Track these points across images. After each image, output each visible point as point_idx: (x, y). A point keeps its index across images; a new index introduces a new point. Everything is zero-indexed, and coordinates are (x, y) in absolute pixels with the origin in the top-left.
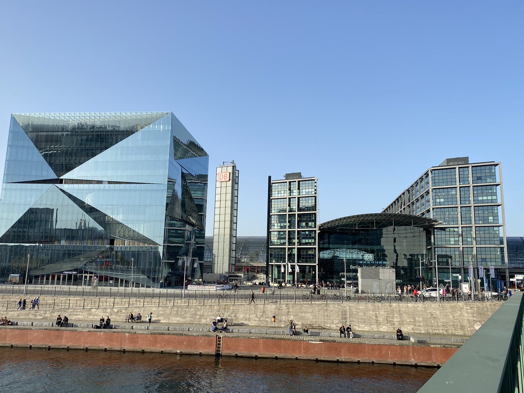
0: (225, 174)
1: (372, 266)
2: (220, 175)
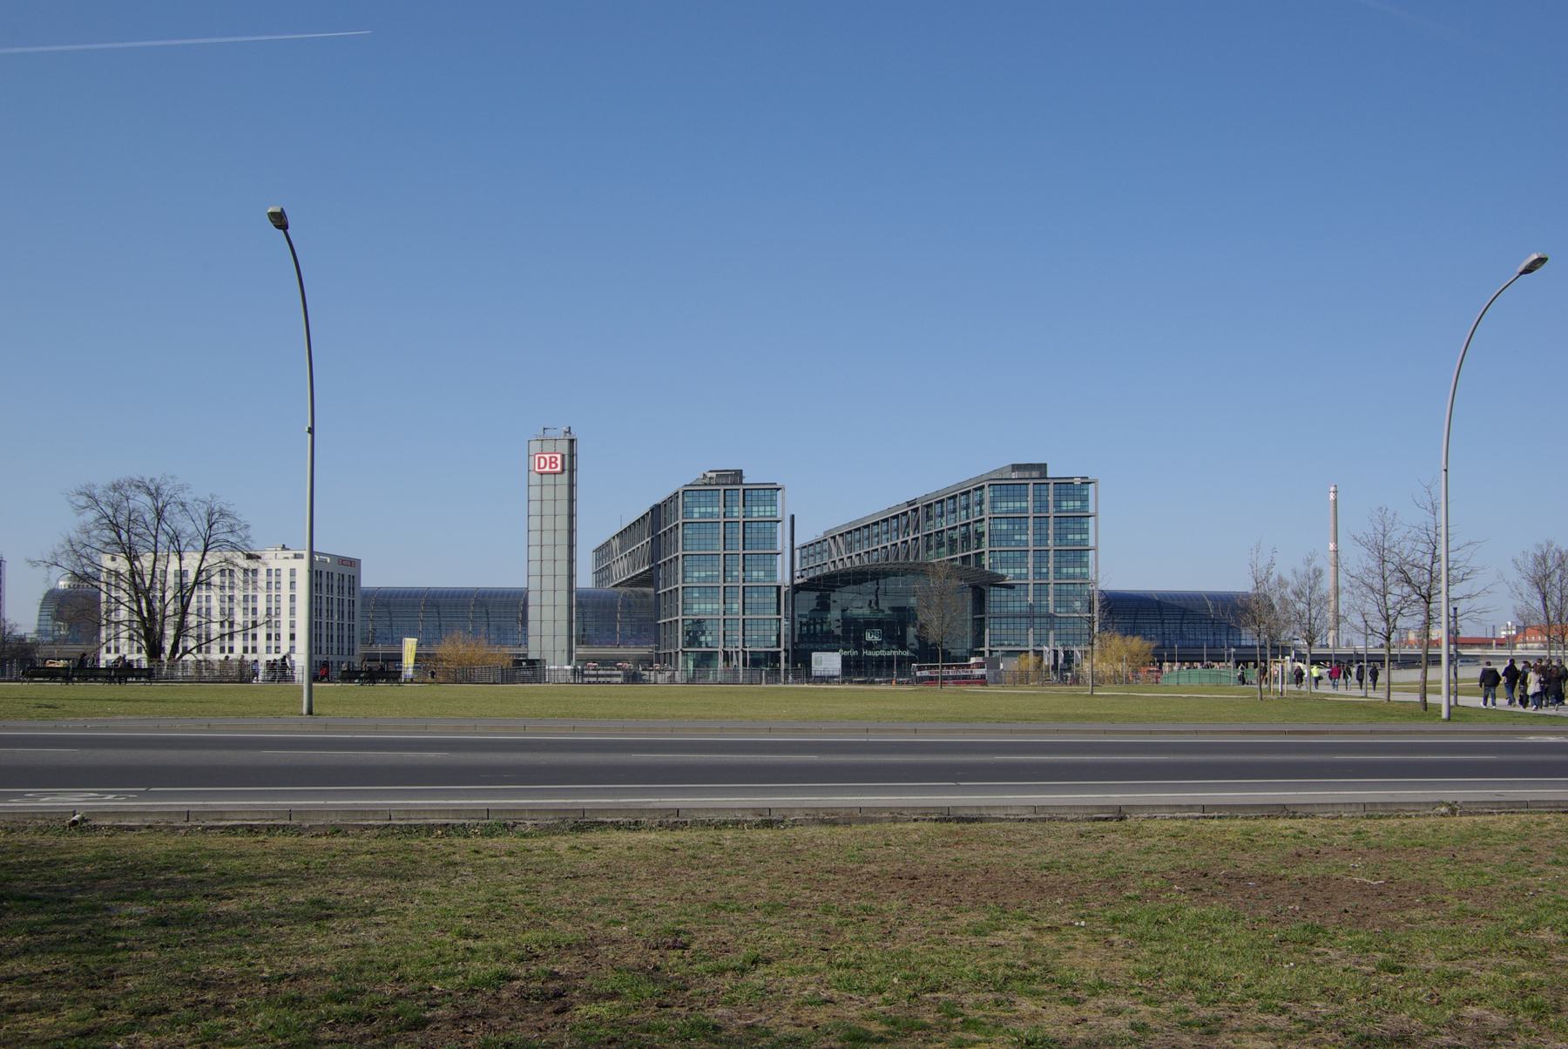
0: (551, 458)
2: (539, 458)
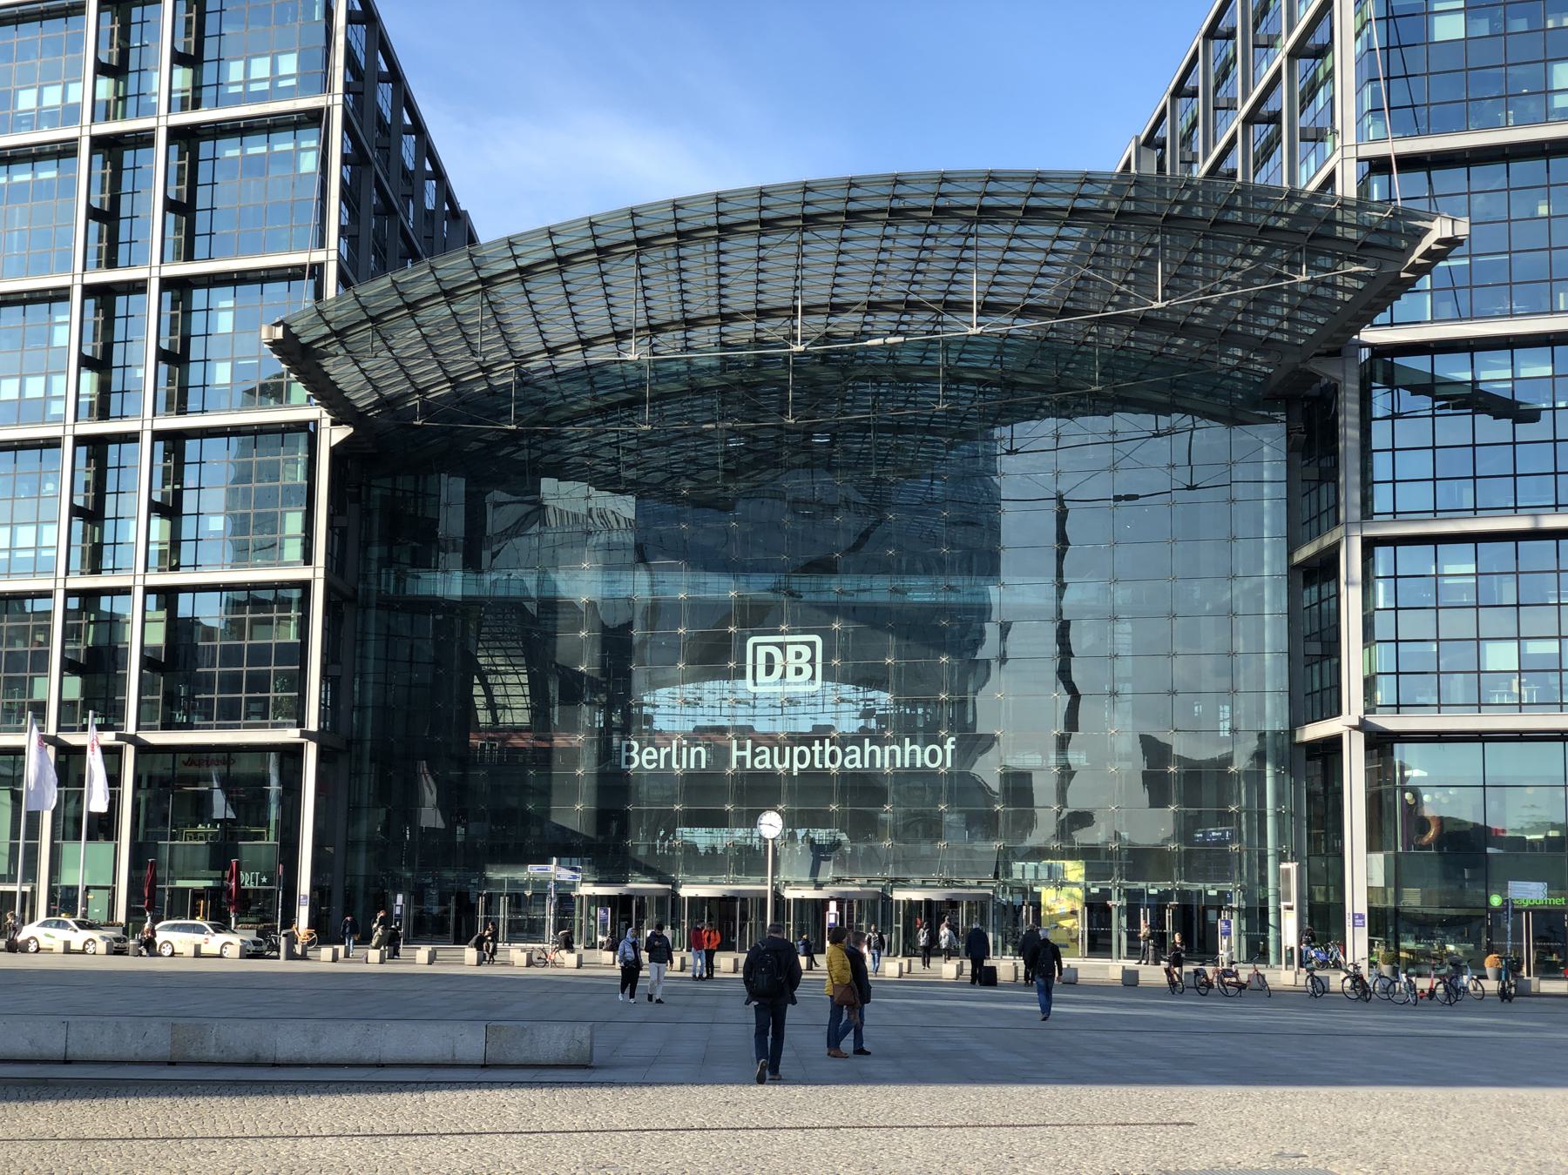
1: (810, 745)
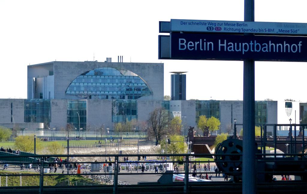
1: (249, 43)
